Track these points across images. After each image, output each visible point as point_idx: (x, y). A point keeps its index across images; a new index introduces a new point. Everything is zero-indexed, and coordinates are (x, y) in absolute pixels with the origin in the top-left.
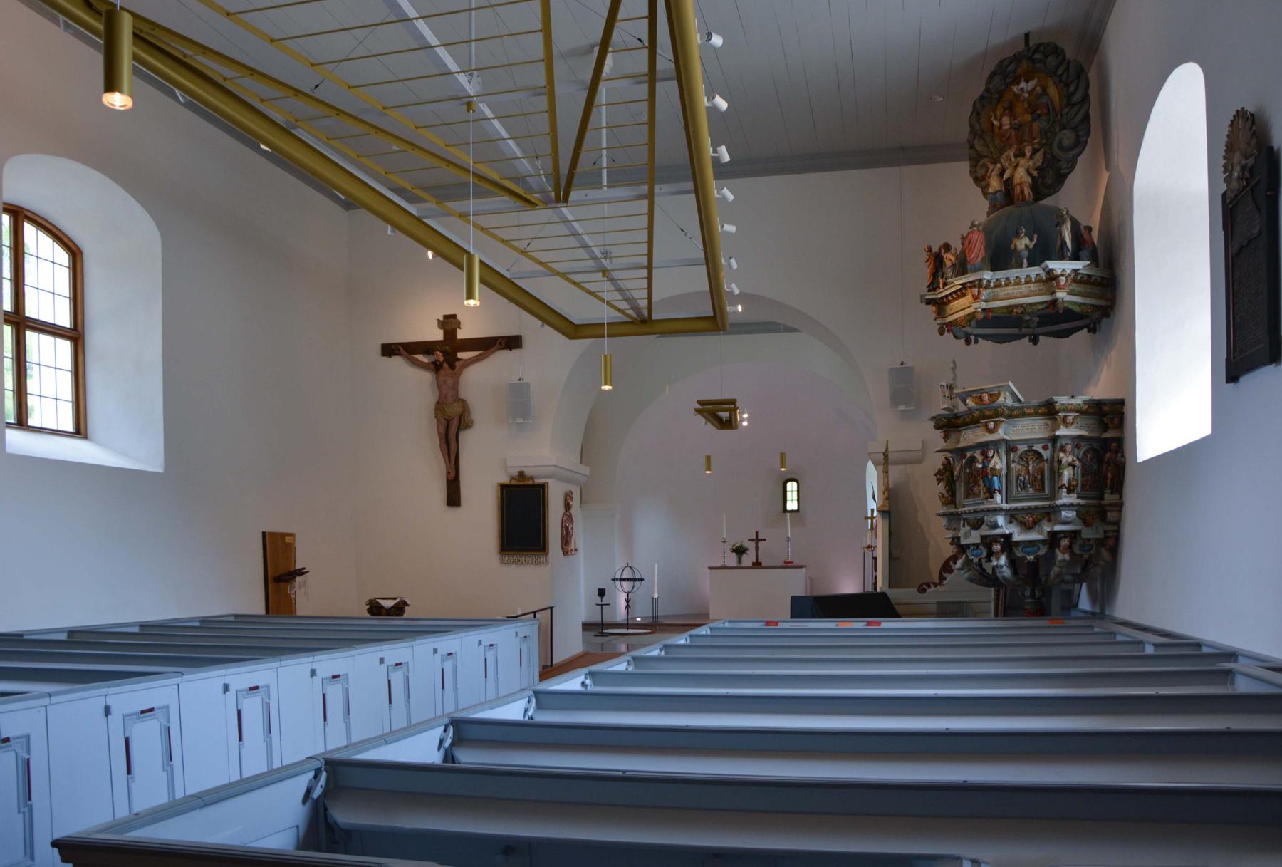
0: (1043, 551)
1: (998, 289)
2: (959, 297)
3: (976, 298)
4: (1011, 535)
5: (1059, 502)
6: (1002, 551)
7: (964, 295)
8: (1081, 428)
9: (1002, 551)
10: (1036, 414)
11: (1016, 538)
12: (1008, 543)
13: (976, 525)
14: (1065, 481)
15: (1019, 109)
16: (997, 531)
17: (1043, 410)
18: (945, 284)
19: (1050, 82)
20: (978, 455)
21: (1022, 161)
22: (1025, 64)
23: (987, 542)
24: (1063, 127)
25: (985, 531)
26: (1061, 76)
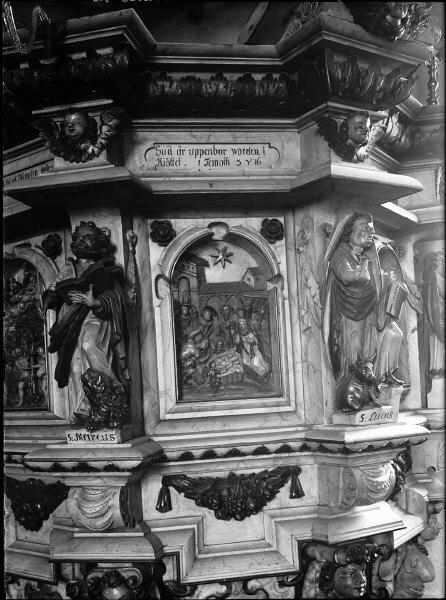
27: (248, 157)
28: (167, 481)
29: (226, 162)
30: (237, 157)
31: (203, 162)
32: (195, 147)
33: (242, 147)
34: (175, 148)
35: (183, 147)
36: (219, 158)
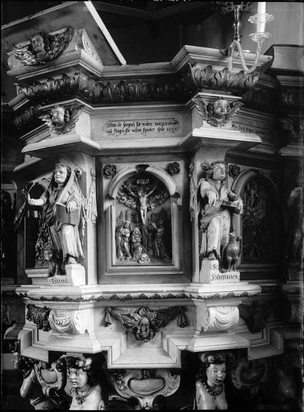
5: (204, 290)
6: (91, 383)
8: (243, 130)
9: (91, 383)
14: (215, 245)
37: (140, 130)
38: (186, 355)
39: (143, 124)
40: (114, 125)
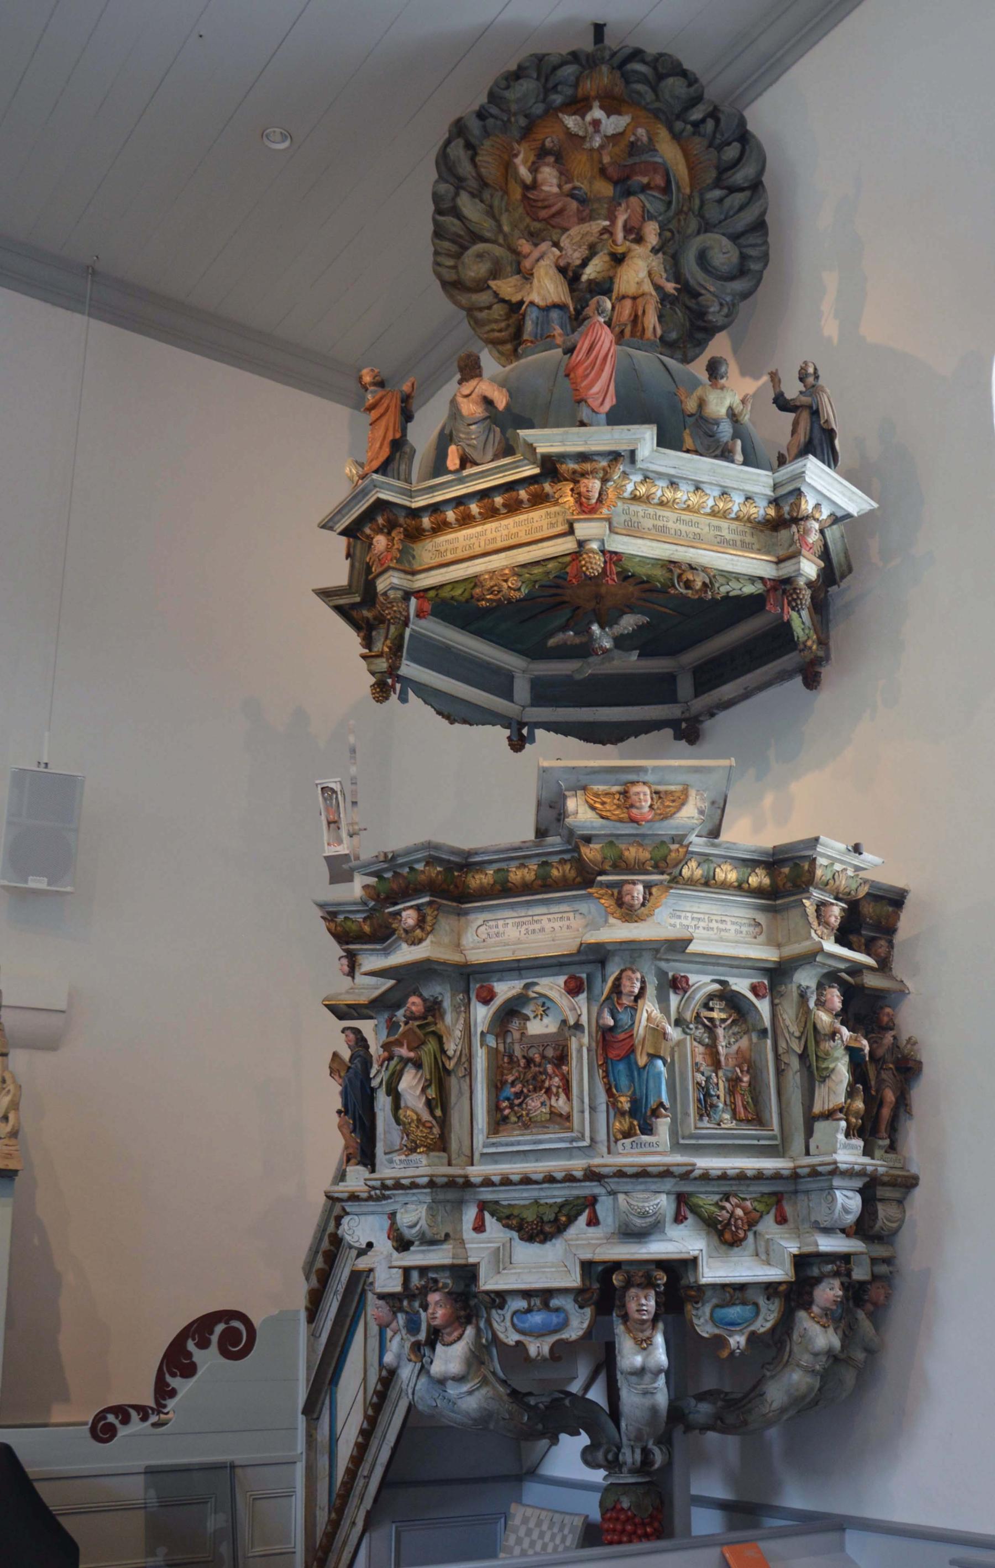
0: (765, 1322)
1: (639, 508)
2: (514, 508)
3: (587, 508)
4: (692, 1263)
7: (539, 500)
10: (740, 887)
11: (714, 1271)
12: (676, 1284)
13: (540, 1228)
15: (580, 164)
16: (657, 1249)
17: (758, 878)
18: (465, 461)
19: (663, 133)
20: (552, 986)
21: (638, 250)
22: (604, 77)
23: (604, 1287)
24: (707, 227)
25: (587, 1242)
26: (696, 124)
27: (560, 924)
28: (483, 1206)
29: (542, 930)
30: (552, 924)
31: (523, 931)
32: (517, 920)
33: (556, 916)
34: (501, 923)
35: (507, 921)
36: (537, 926)
37: (712, 929)
38: (801, 1261)
39: (717, 921)
40: (679, 917)
